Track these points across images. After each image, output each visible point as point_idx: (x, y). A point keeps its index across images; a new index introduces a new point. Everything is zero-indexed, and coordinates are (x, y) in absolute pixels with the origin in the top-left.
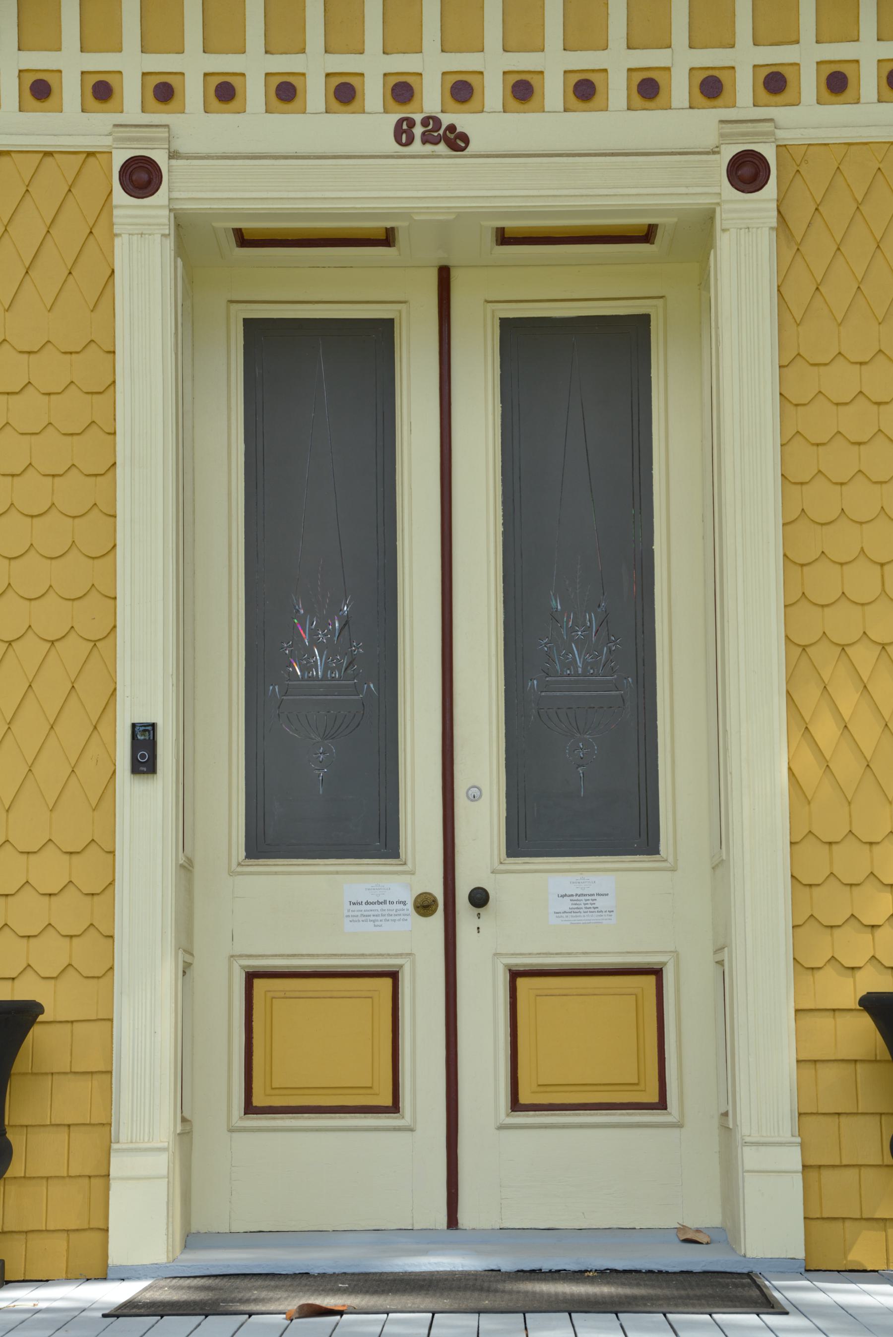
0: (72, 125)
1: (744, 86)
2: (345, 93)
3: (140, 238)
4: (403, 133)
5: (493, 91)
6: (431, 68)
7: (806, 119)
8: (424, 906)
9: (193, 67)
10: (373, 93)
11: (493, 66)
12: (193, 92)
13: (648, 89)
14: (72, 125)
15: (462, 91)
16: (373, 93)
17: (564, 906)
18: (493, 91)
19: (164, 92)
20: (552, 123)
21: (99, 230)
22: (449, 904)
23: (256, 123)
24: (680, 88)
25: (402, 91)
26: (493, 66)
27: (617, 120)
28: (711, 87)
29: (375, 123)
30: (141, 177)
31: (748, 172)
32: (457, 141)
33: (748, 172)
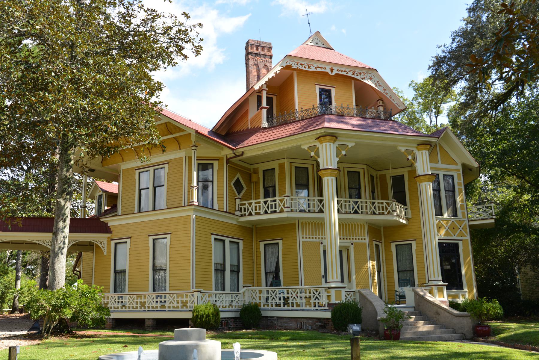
3: (322, 246)
14: (318, 240)
27: (345, 241)
30: (322, 243)
31: (352, 244)
33: (352, 244)
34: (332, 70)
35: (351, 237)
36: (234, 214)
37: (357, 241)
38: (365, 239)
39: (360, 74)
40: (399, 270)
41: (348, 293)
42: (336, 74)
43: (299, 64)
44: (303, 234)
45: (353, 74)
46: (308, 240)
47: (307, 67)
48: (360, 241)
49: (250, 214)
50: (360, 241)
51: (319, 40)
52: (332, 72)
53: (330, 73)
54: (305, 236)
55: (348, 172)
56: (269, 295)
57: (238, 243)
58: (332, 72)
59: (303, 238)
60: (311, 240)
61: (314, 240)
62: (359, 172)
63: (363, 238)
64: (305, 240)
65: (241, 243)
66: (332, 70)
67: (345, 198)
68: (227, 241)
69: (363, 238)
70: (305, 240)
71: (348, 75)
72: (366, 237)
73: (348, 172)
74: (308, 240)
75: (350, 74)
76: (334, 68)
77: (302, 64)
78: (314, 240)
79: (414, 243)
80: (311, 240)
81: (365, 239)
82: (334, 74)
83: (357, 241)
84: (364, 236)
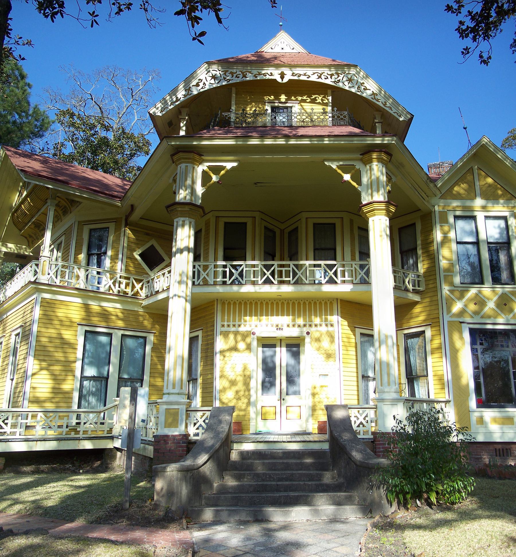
34: (282, 75)
39: (332, 75)
42: (290, 80)
43: (227, 74)
45: (320, 77)
47: (241, 76)
51: (286, 43)
52: (282, 77)
53: (279, 80)
54: (226, 323)
55: (314, 224)
58: (282, 77)
59: (223, 326)
62: (334, 224)
66: (282, 75)
67: (282, 259)
71: (310, 79)
73: (314, 224)
75: (314, 78)
76: (285, 72)
77: (232, 73)
82: (285, 80)
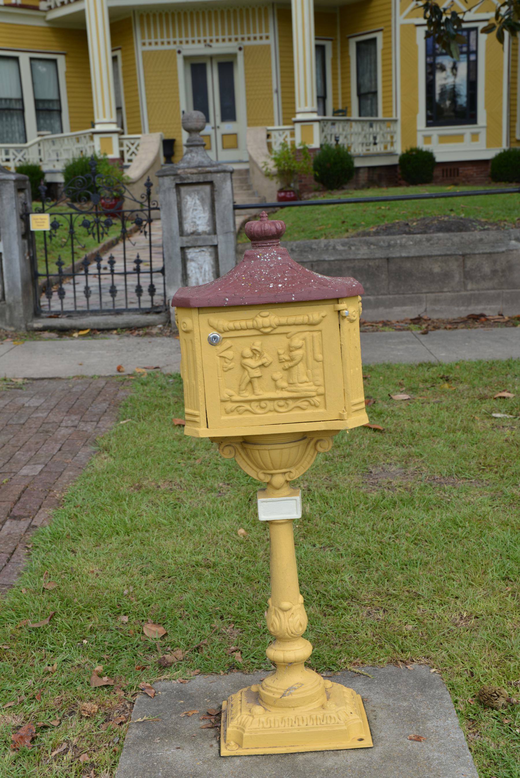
0: (172, 47)
1: (240, 39)
2: (199, 41)
4: (205, 46)
5: (214, 41)
6: (208, 38)
7: (246, 43)
8: (213, 128)
9: (184, 39)
10: (202, 41)
11: (214, 38)
12: (184, 42)
13: (230, 40)
14: (172, 47)
15: (211, 41)
16: (202, 41)
17: (228, 127)
18: (214, 41)
19: (181, 42)
20: (221, 44)
21: (175, 58)
22: (215, 128)
23: (191, 45)
24: (233, 40)
25: (205, 41)
26: (214, 38)
27: (227, 44)
28: (236, 39)
29: (202, 45)
30: (179, 52)
31: (240, 49)
32: (210, 46)
33: (240, 49)
35: (239, 36)
36: (36, 8)
37: (252, 42)
38: (267, 38)
40: (363, 91)
41: (132, 141)
44: (143, 37)
46: (153, 47)
48: (258, 42)
49: (56, 7)
50: (258, 42)
54: (147, 41)
56: (125, 149)
57: (55, 61)
59: (144, 44)
60: (160, 47)
61: (166, 47)
63: (264, 35)
64: (147, 48)
65: (61, 60)
68: (24, 59)
69: (264, 35)
70: (147, 48)
72: (271, 34)
74: (153, 47)
78: (166, 47)
79: (379, 36)
80: (160, 47)
81: (267, 38)
83: (252, 42)
84: (267, 31)
